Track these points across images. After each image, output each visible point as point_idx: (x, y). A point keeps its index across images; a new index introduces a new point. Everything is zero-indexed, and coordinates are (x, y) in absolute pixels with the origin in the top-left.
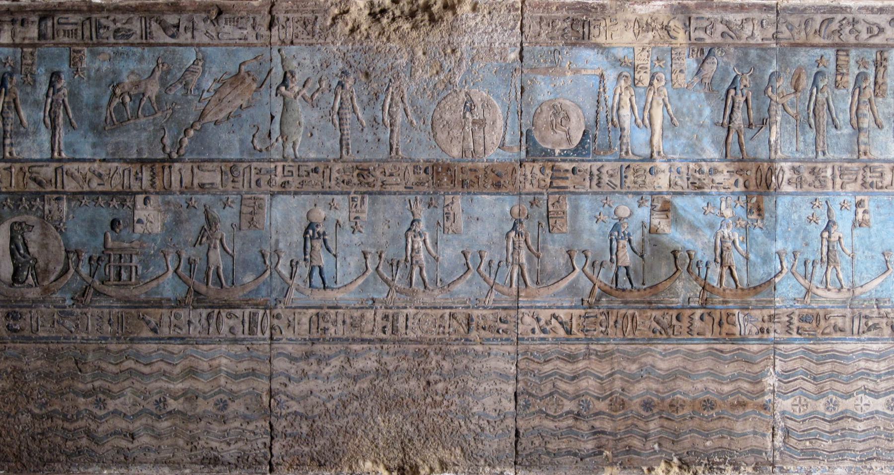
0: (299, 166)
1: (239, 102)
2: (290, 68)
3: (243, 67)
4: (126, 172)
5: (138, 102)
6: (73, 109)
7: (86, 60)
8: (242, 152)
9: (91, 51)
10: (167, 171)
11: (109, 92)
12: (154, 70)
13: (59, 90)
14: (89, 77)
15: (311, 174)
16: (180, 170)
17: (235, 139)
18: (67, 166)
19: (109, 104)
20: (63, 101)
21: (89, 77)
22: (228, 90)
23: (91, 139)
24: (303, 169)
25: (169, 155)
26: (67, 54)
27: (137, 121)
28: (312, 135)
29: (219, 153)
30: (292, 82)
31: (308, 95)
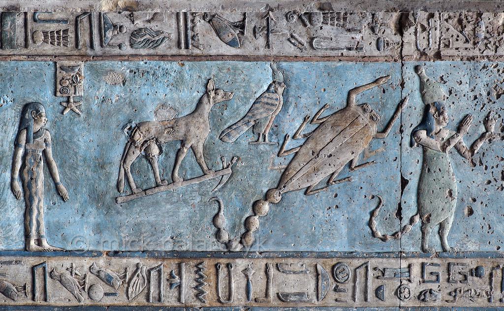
0: (449, 264)
1: (346, 157)
2: (436, 100)
3: (354, 97)
4: (154, 274)
5: (173, 155)
6: (60, 166)
7: (83, 83)
8: (352, 242)
9: (91, 68)
10: (223, 273)
11: (123, 139)
12: (200, 102)
13: (37, 134)
14: (89, 113)
15: (469, 277)
16: (245, 271)
17: (340, 219)
18: (52, 263)
19: (124, 158)
20: (44, 152)
21: (89, 113)
22: (329, 136)
23: (94, 216)
24: (455, 269)
25: (228, 245)
26: (50, 72)
27: (172, 188)
28: (471, 212)
29: (313, 240)
30: (439, 123)
31: (466, 145)
